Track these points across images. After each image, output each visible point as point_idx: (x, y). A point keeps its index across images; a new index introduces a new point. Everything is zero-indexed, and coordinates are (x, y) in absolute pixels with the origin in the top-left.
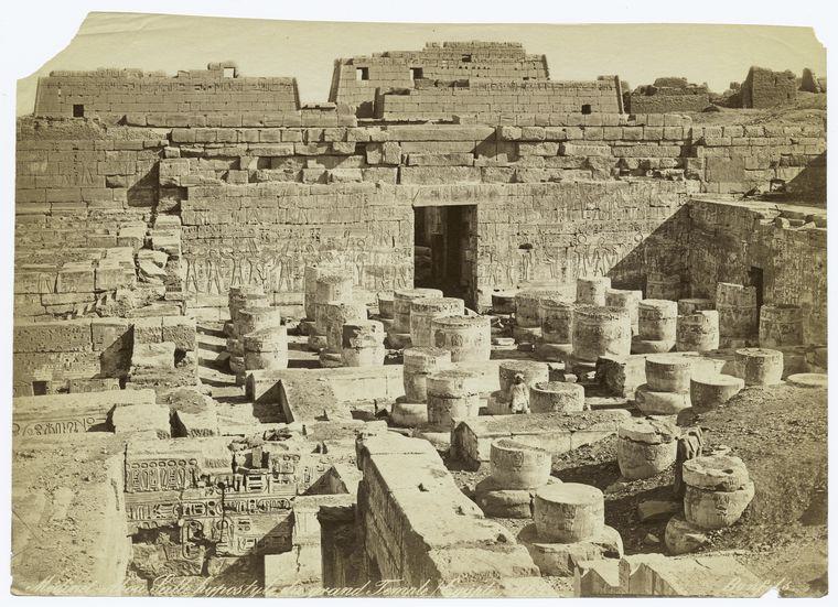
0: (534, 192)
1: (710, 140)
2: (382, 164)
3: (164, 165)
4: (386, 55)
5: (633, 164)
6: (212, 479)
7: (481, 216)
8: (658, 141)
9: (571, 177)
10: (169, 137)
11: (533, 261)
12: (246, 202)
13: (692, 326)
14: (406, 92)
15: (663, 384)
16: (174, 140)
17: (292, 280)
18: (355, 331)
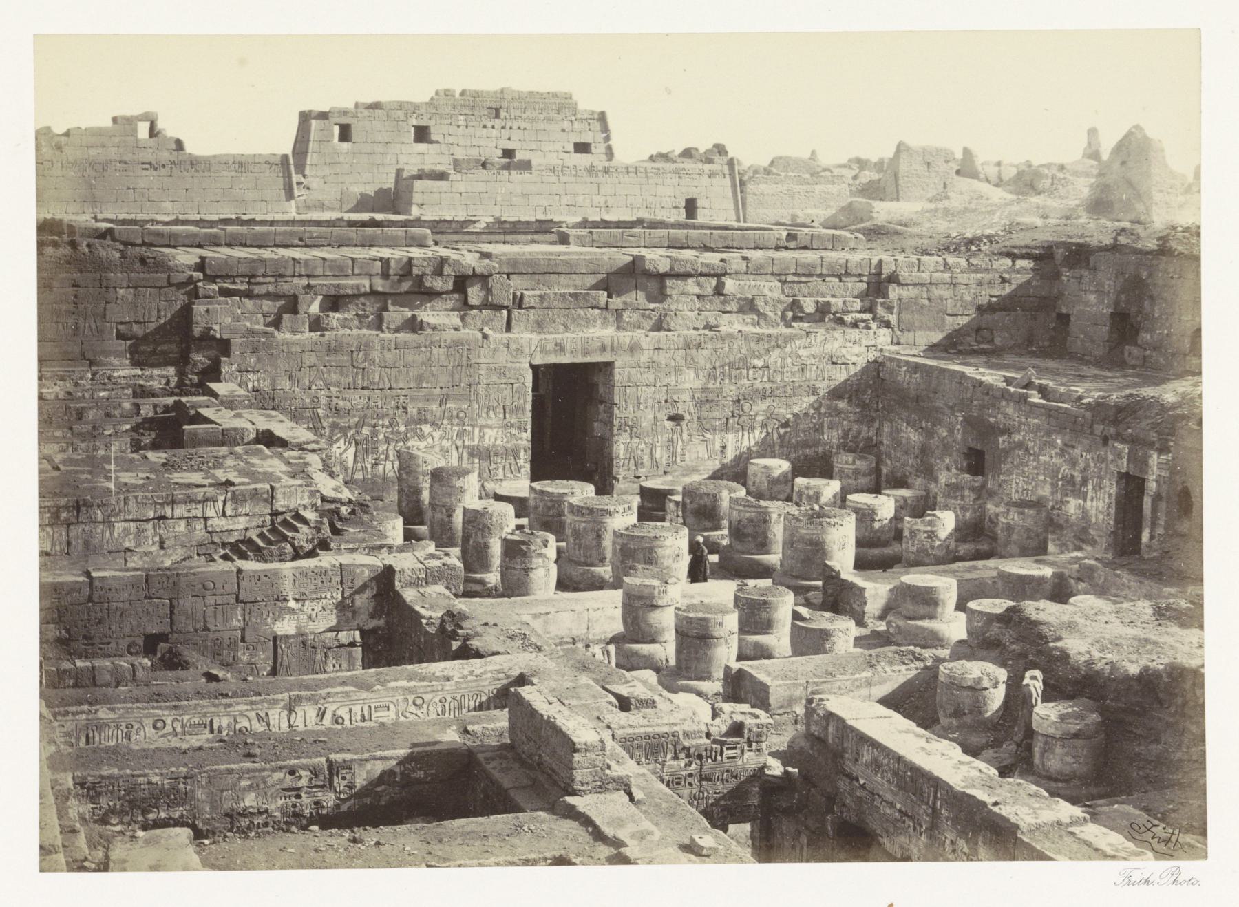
0: (687, 345)
1: (904, 275)
2: (486, 305)
3: (199, 308)
4: (376, 106)
5: (809, 306)
6: (692, 751)
7: (619, 375)
8: (839, 276)
9: (733, 324)
10: (201, 266)
11: (685, 436)
12: (310, 359)
13: (925, 532)
14: (442, 176)
15: (922, 610)
16: (208, 272)
17: (369, 466)
18: (524, 547)
